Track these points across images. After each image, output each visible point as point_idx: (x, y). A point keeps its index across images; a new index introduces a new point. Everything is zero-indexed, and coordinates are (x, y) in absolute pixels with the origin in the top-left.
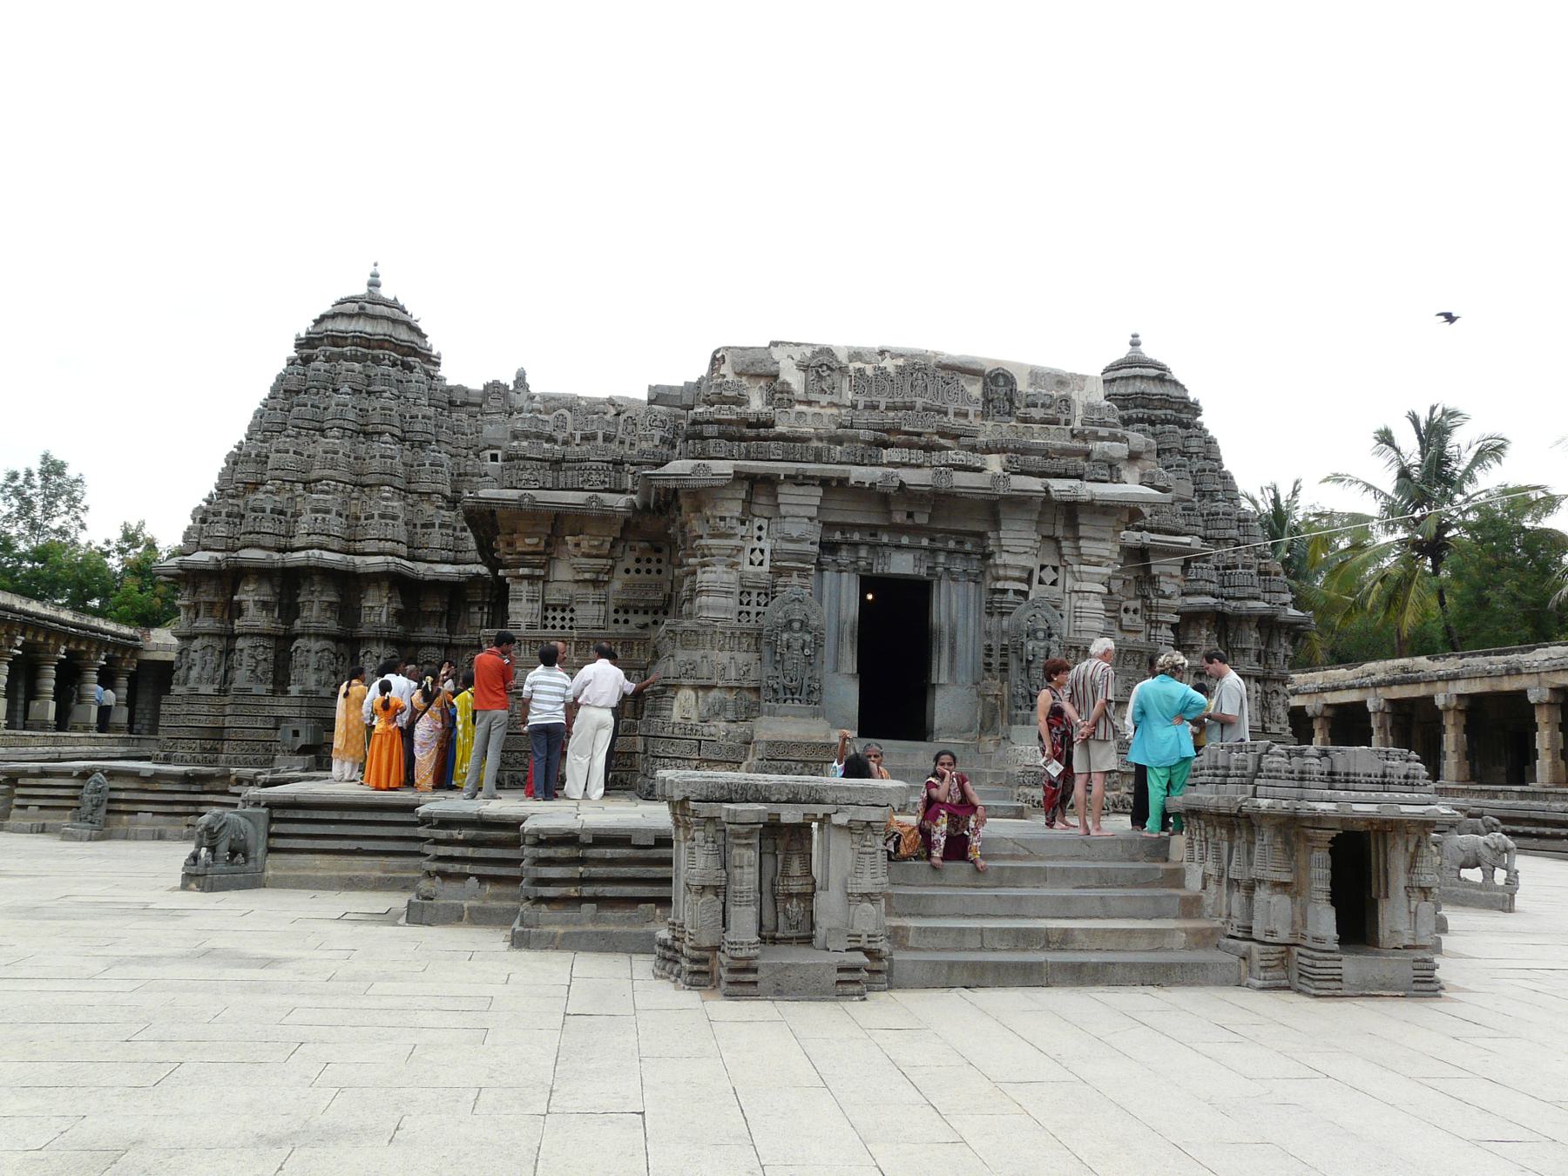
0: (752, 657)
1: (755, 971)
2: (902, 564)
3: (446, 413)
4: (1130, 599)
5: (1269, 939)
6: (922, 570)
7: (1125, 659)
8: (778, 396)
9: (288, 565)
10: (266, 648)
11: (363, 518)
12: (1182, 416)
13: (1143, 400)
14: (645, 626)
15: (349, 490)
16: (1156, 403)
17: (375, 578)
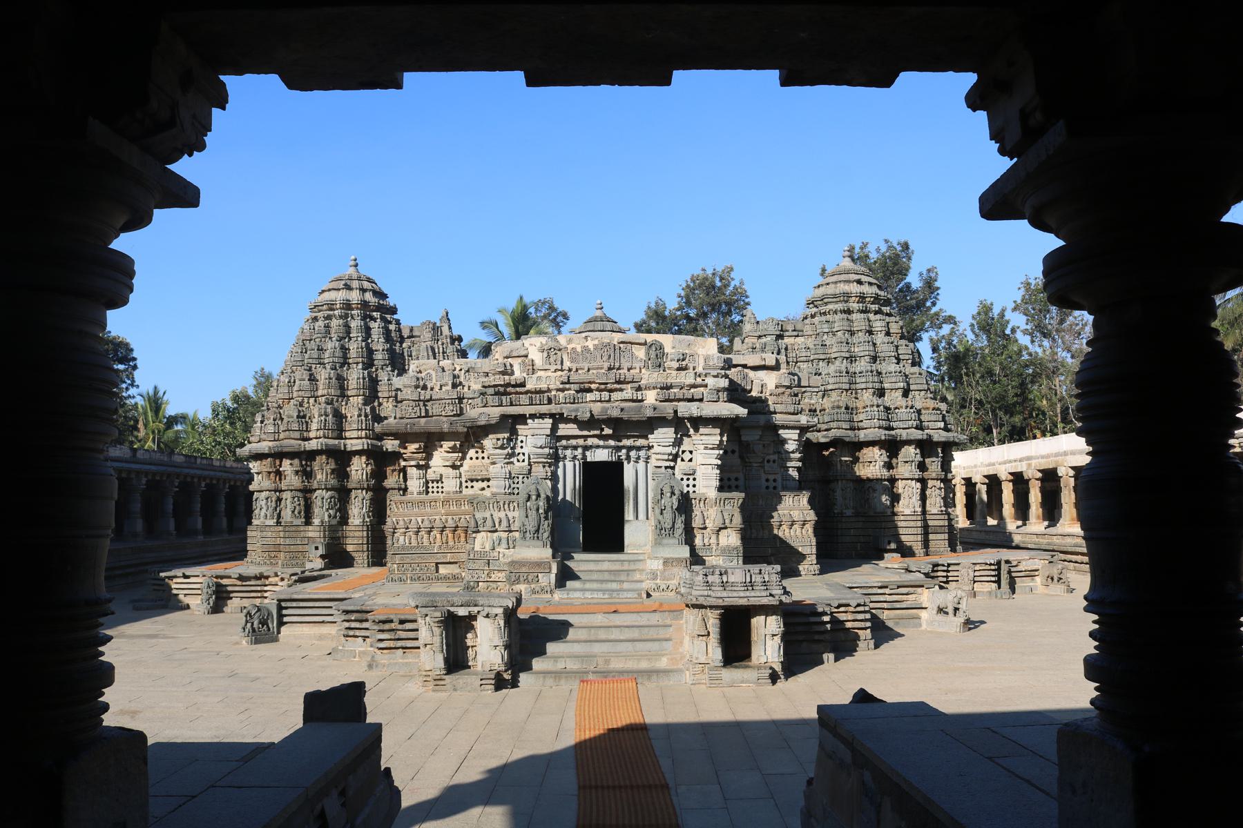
0: (516, 514)
1: (444, 680)
2: (601, 455)
3: (398, 344)
4: (770, 454)
5: (696, 662)
6: (614, 458)
7: (724, 503)
8: (527, 368)
9: (307, 449)
10: (299, 497)
11: (349, 417)
12: (874, 306)
13: (846, 297)
14: (483, 489)
15: (340, 400)
16: (854, 298)
17: (359, 453)
